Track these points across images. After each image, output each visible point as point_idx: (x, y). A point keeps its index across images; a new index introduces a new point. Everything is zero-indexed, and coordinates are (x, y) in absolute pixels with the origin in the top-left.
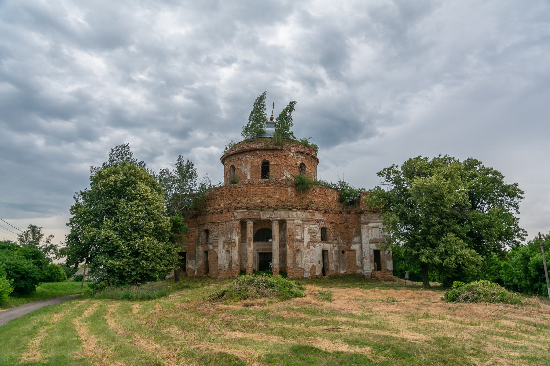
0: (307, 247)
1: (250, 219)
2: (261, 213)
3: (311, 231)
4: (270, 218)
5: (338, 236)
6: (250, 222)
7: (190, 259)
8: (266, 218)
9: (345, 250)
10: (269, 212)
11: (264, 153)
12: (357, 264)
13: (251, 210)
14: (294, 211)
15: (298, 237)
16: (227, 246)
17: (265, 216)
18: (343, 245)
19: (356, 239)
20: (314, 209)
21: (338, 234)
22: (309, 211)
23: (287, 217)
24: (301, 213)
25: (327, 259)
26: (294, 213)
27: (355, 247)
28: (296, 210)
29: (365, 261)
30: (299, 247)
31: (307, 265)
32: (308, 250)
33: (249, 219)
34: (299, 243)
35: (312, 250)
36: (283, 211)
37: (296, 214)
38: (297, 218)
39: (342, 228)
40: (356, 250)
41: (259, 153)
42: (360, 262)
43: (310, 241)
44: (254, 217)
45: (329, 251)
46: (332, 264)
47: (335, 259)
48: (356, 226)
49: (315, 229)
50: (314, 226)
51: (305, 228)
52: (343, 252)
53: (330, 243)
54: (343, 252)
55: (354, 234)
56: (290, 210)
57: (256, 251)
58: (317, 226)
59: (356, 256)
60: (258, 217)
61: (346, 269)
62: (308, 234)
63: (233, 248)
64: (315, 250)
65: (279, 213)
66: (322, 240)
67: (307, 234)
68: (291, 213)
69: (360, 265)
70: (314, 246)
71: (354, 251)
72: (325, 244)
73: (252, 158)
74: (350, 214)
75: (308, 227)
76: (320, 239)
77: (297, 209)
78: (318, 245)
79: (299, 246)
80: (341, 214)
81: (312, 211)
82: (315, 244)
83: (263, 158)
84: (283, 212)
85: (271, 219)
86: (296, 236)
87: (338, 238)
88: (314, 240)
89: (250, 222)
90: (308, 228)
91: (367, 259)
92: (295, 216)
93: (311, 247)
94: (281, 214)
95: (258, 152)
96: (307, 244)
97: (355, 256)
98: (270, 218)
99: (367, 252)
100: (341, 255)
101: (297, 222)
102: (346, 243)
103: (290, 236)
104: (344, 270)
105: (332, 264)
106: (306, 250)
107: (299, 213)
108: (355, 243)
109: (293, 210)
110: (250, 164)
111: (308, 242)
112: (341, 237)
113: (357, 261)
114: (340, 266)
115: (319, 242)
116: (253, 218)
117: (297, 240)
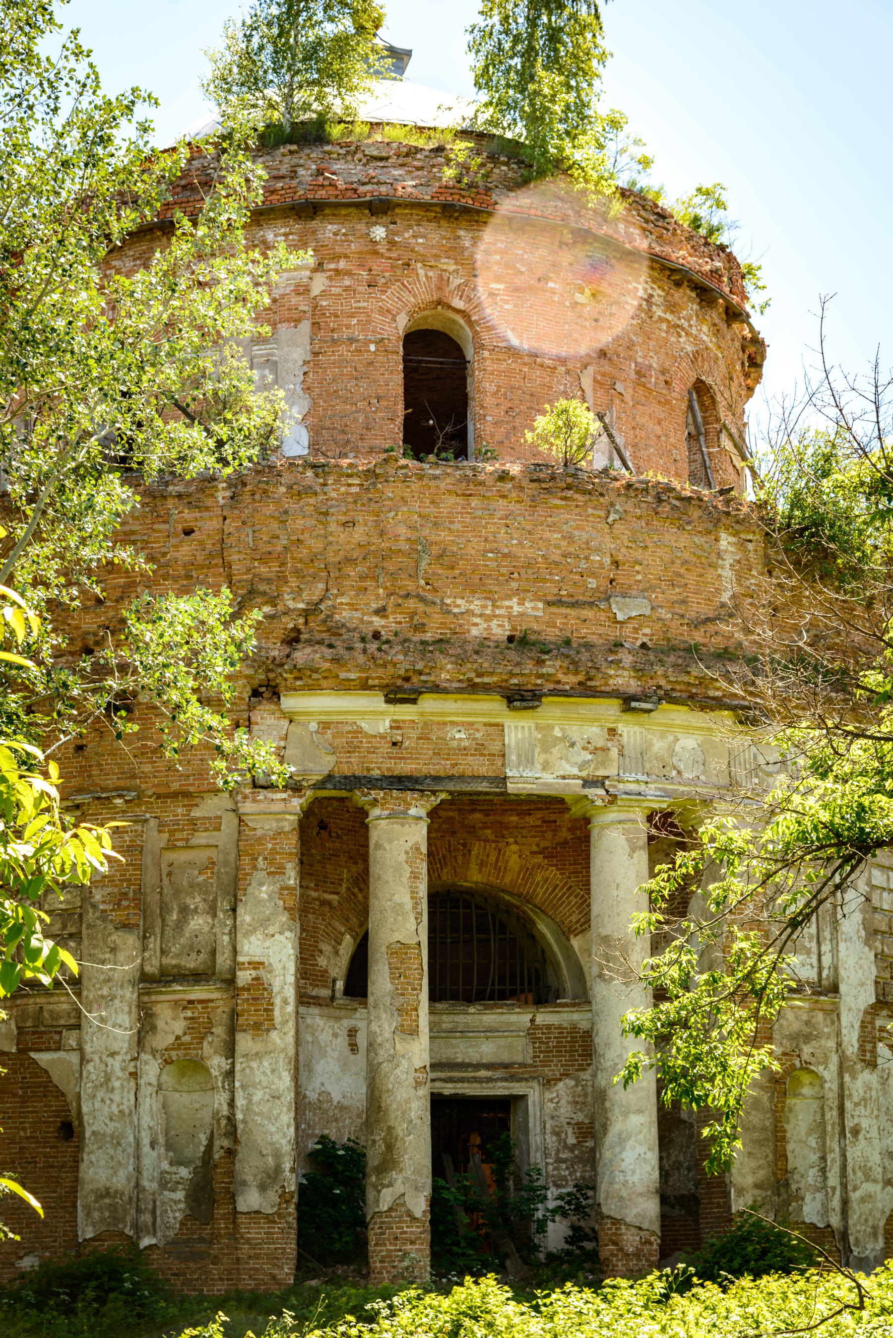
8: (548, 778)
10: (577, 732)
16: (179, 1027)
17: (546, 766)
30: (807, 1050)
31: (863, 1200)
60: (480, 766)
63: (245, 1042)
67: (859, 945)
73: (319, 284)
79: (808, 1038)
94: (672, 752)
95: (379, 232)
98: (588, 783)
106: (854, 1077)
110: (305, 326)
116: (437, 779)
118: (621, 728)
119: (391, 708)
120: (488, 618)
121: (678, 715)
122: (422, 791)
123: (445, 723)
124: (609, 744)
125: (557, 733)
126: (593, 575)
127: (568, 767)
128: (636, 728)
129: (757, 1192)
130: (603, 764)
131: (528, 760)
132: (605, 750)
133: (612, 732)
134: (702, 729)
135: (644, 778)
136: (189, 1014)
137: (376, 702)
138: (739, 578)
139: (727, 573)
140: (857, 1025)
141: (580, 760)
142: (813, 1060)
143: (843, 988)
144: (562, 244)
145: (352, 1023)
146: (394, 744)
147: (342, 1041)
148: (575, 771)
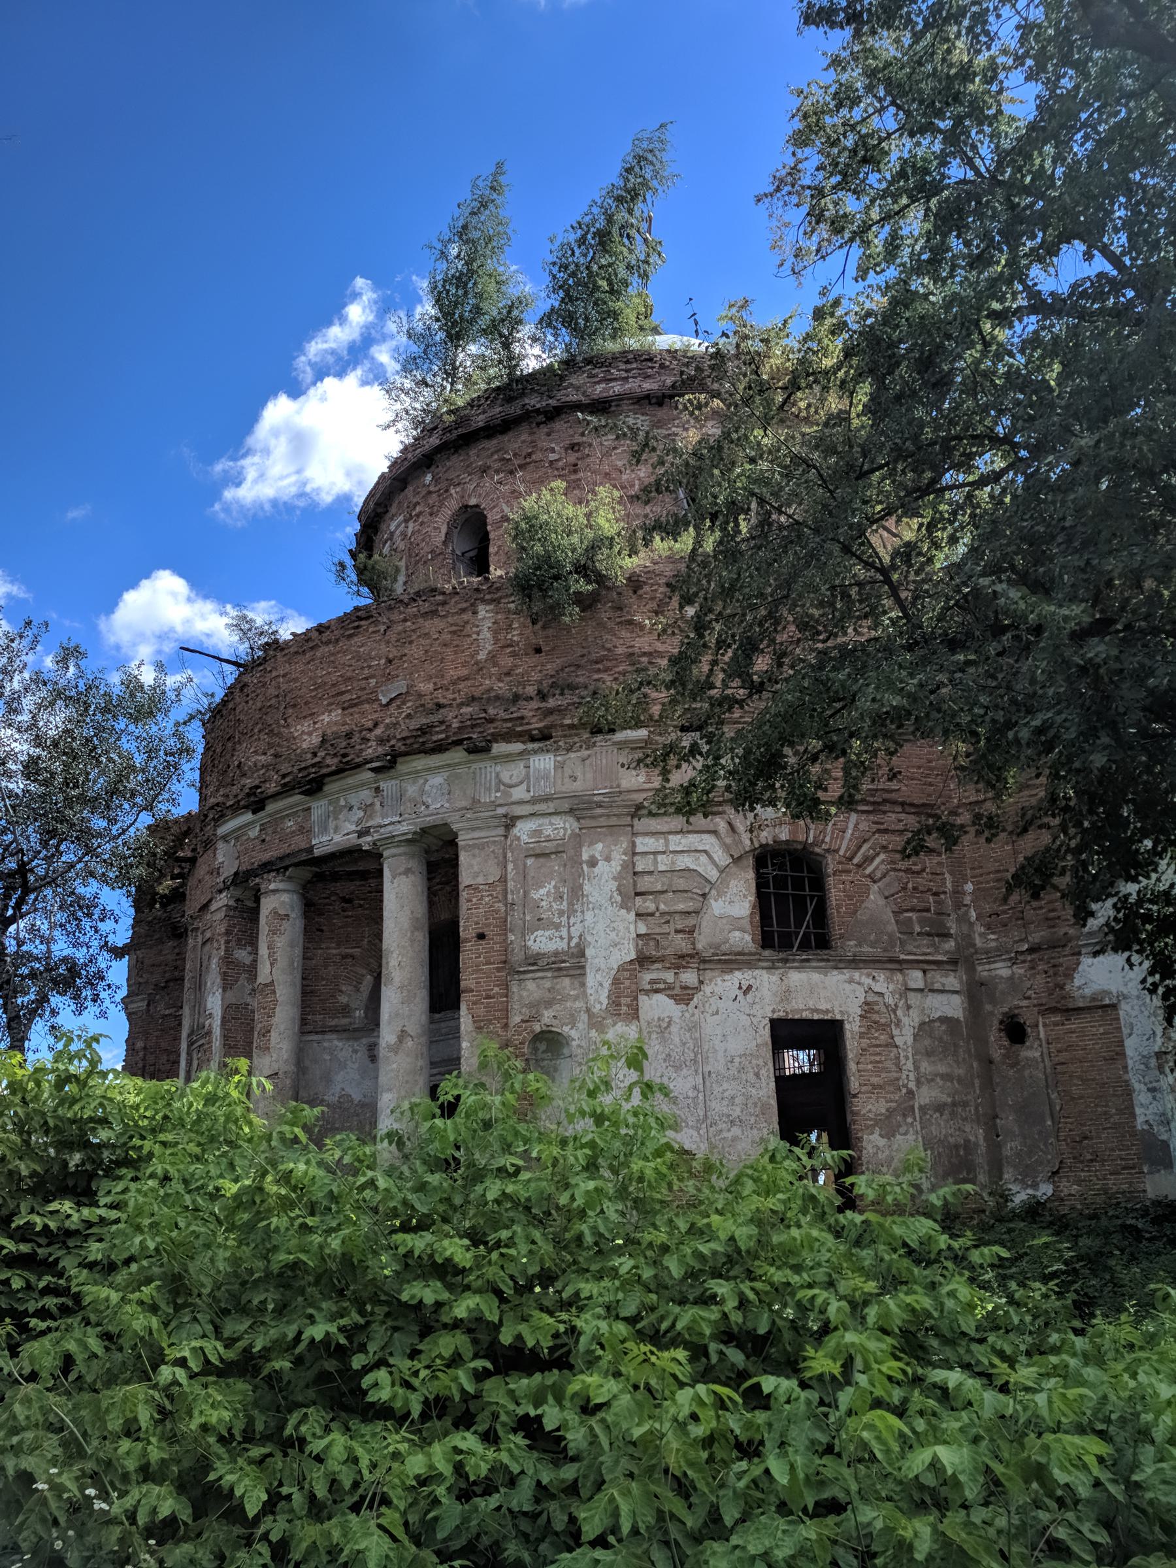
0: (615, 1002)
1: (267, 867)
2: (319, 807)
3: (645, 883)
4: (361, 834)
5: (959, 905)
8: (338, 838)
10: (354, 799)
13: (271, 807)
14: (509, 758)
15: (543, 942)
18: (1005, 972)
21: (958, 892)
22: (620, 736)
23: (464, 804)
24: (560, 766)
26: (512, 772)
28: (517, 747)
32: (620, 1027)
34: (548, 984)
35: (663, 1028)
36: (431, 770)
37: (527, 776)
38: (534, 801)
41: (436, 480)
43: (643, 960)
44: (284, 849)
45: (852, 1028)
46: (889, 1134)
47: (926, 1096)
49: (685, 862)
50: (677, 842)
51: (593, 863)
52: (1016, 1032)
53: (855, 963)
54: (1016, 1032)
56: (479, 750)
58: (708, 842)
59: (1122, 1054)
60: (299, 842)
62: (624, 906)
64: (694, 1027)
65: (411, 790)
66: (766, 941)
68: (487, 769)
70: (684, 996)
72: (796, 977)
75: (619, 857)
76: (744, 939)
77: (533, 739)
78: (725, 984)
79: (549, 1004)
81: (643, 733)
82: (689, 977)
83: (452, 505)
84: (437, 780)
85: (366, 842)
86: (526, 930)
87: (963, 919)
89: (272, 886)
90: (615, 866)
92: (519, 793)
93: (657, 1006)
95: (429, 478)
96: (616, 982)
98: (361, 834)
100: (997, 1054)
101: (536, 833)
102: (1031, 950)
103: (481, 936)
105: (889, 1134)
107: (544, 763)
109: (499, 748)
111: (621, 968)
114: (995, 1147)
115: (730, 961)
116: (281, 859)
117: (534, 960)
118: (383, 785)
120: (310, 734)
121: (420, 762)
123: (283, 818)
125: (342, 802)
126: (372, 677)
130: (371, 817)
131: (325, 829)
132: (372, 804)
133: (377, 790)
134: (442, 767)
135: (397, 818)
137: (248, 817)
138: (495, 633)
139: (486, 634)
140: (607, 984)
141: (355, 818)
142: (555, 1022)
143: (589, 952)
144: (538, 424)
147: (362, 1055)
148: (353, 828)
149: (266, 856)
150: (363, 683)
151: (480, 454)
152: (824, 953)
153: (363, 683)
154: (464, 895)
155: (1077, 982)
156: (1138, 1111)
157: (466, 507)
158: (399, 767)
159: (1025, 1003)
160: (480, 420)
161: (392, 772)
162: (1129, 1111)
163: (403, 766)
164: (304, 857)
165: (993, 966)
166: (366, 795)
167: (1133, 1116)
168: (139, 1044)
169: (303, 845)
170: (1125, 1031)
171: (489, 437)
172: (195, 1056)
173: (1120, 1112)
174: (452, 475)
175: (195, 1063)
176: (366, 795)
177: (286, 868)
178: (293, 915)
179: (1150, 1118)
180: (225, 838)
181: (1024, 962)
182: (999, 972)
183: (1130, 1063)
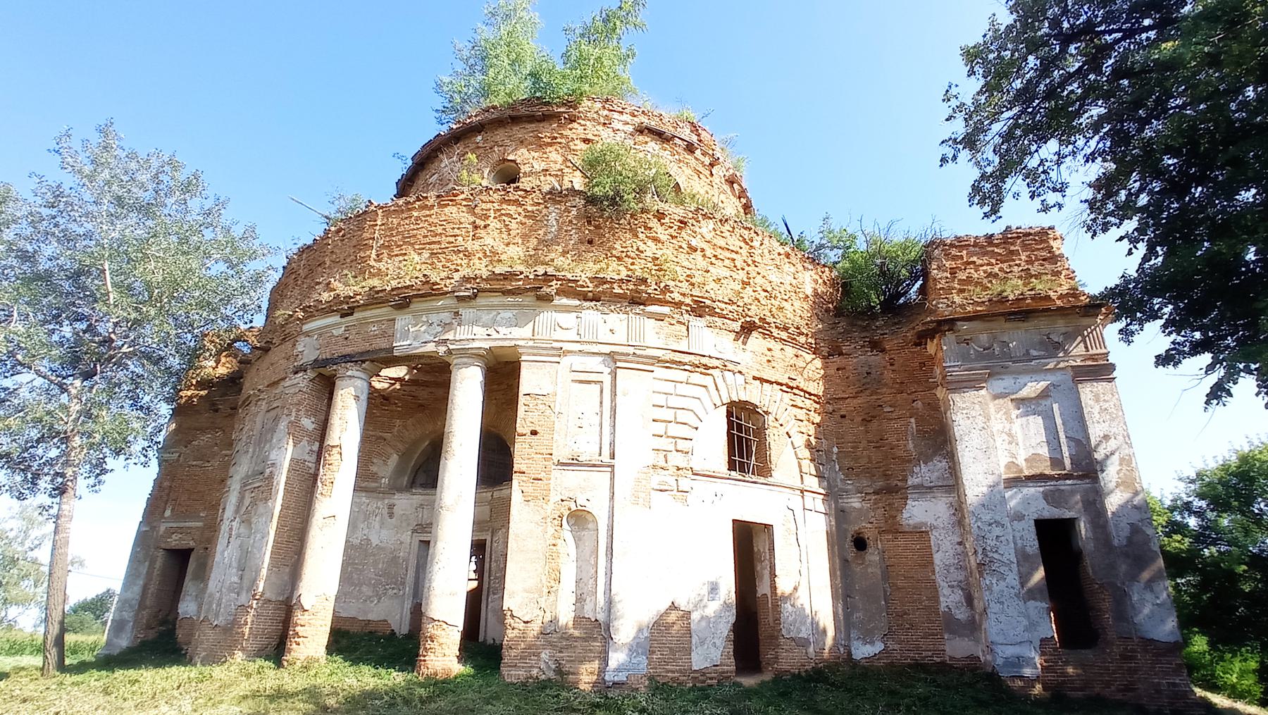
1: (348, 359)
2: (403, 321)
6: (349, 373)
7: (192, 579)
8: (416, 344)
9: (869, 534)
10: (434, 318)
11: (500, 135)
12: (943, 607)
13: (357, 315)
14: (567, 310)
19: (925, 473)
20: (678, 305)
25: (766, 573)
26: (568, 319)
27: (917, 511)
29: (989, 588)
33: (345, 356)
36: (505, 307)
39: (846, 421)
40: (933, 527)
41: (485, 141)
42: (958, 596)
48: (919, 404)
50: (682, 389)
52: (860, 544)
54: (860, 544)
55: (911, 446)
57: (414, 531)
60: (383, 344)
61: (884, 638)
66: (732, 466)
69: (961, 614)
71: (921, 533)
74: (883, 350)
80: (841, 354)
81: (666, 310)
83: (496, 157)
88: (677, 459)
89: (349, 373)
91: (1002, 577)
95: (479, 138)
97: (928, 562)
99: (997, 531)
103: (534, 433)
104: (872, 643)
108: (925, 490)
112: (847, 463)
113: (944, 591)
116: (362, 353)
119: (343, 320)
121: (497, 300)
122: (357, 361)
123: (368, 323)
124: (454, 321)
125: (424, 319)
127: (428, 337)
128: (471, 310)
129: (525, 595)
133: (457, 313)
136: (253, 495)
137: (335, 319)
141: (435, 332)
145: (392, 501)
146: (346, 338)
149: (348, 350)
150: (452, 239)
151: (518, 131)
152: (762, 480)
153: (452, 239)
154: (522, 400)
155: (905, 515)
156: (942, 599)
157: (505, 160)
158: (478, 300)
159: (870, 526)
160: (523, 111)
161: (473, 303)
162: (935, 598)
163: (481, 301)
164: (383, 355)
165: (849, 500)
166: (446, 317)
167: (938, 602)
168: (166, 484)
169: (384, 346)
170: (934, 549)
171: (531, 122)
172: (248, 495)
173: (929, 599)
174: (498, 138)
175: (247, 501)
176: (446, 317)
177: (363, 362)
178: (362, 398)
179: (950, 604)
180: (307, 334)
181: (870, 500)
182: (854, 505)
183: (937, 569)
